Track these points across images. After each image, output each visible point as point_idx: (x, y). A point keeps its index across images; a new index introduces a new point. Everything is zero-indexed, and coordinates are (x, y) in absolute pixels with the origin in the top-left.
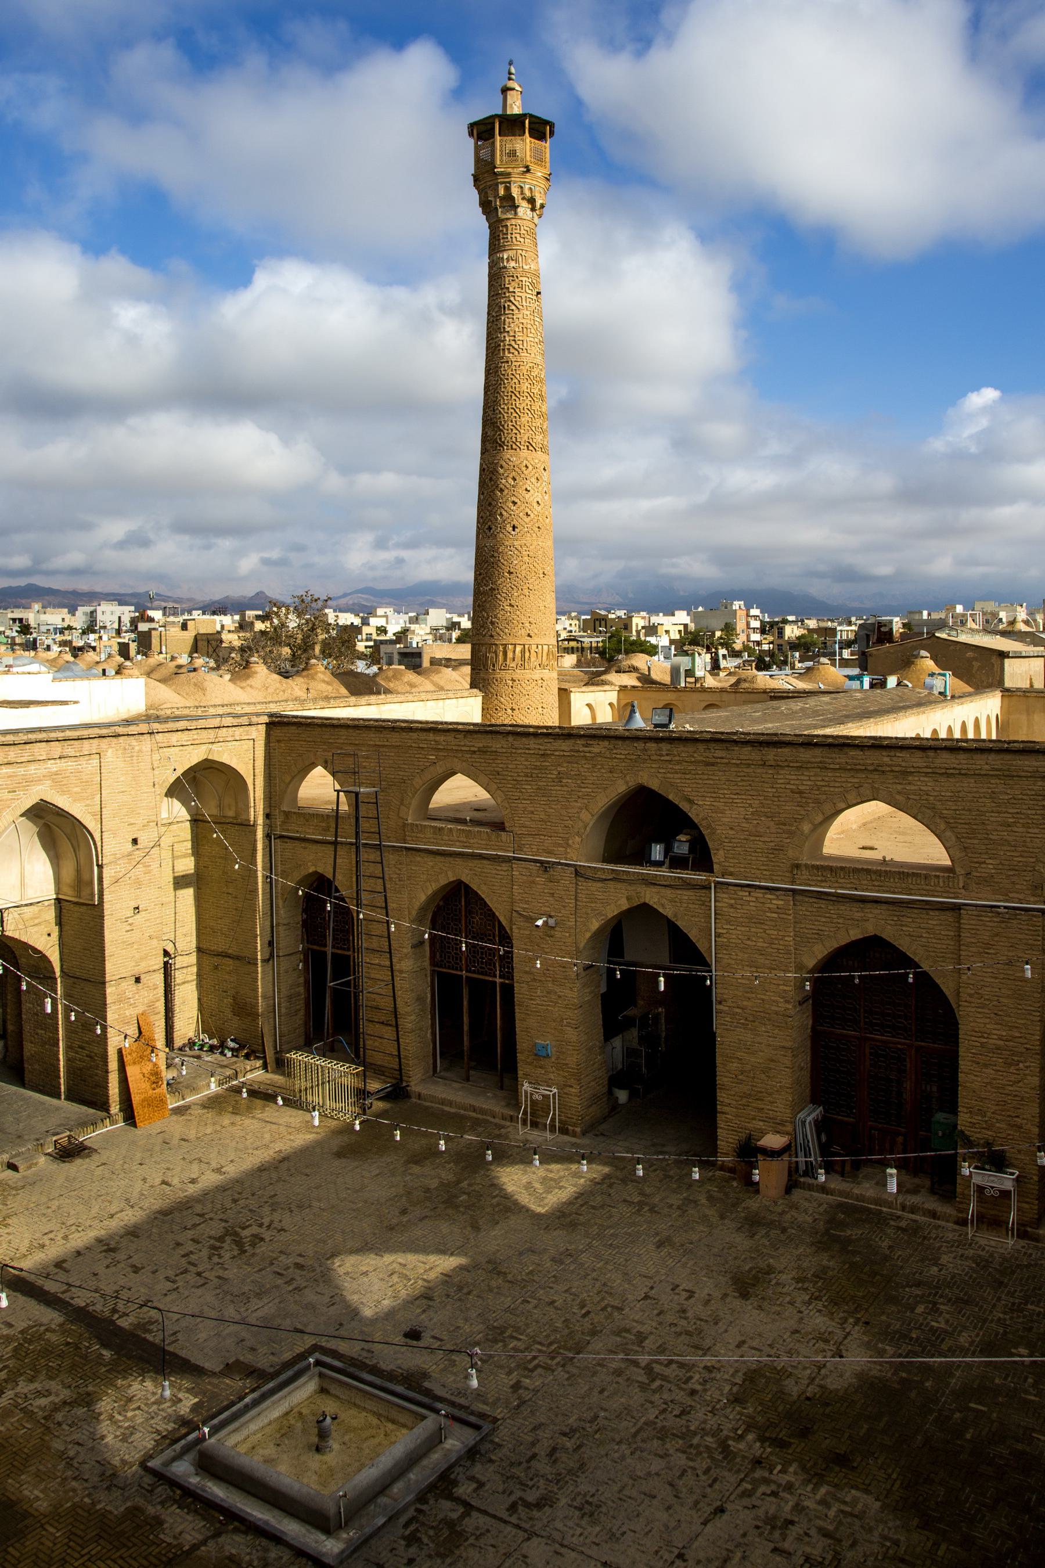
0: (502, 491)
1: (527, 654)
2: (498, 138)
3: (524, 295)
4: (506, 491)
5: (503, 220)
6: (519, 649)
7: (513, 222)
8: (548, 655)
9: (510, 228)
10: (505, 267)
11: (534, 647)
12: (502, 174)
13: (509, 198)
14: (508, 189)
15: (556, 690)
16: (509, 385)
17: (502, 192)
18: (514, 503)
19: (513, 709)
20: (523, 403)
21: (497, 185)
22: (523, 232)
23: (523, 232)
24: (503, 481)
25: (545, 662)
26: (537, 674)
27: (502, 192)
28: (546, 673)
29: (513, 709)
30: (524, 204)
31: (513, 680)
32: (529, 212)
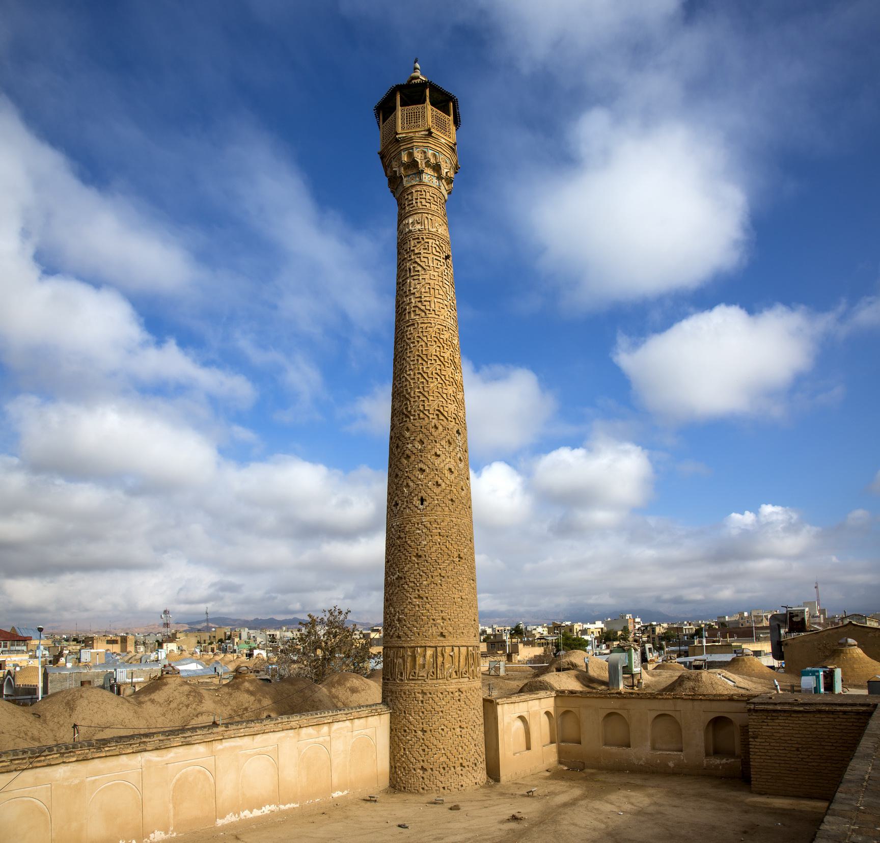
0: (408, 457)
1: (440, 659)
2: (399, 108)
3: (430, 256)
4: (413, 457)
5: (408, 188)
6: (429, 652)
7: (418, 188)
8: (467, 659)
9: (415, 194)
10: (410, 231)
11: (448, 650)
12: (405, 140)
13: (413, 164)
14: (411, 155)
15: (480, 703)
16: (415, 349)
17: (405, 158)
18: (422, 471)
19: (424, 731)
20: (432, 368)
21: (400, 153)
22: (428, 197)
23: (428, 197)
24: (410, 446)
25: (463, 668)
26: (453, 685)
27: (405, 158)
28: (465, 683)
29: (424, 731)
30: (429, 171)
31: (424, 693)
32: (435, 180)
